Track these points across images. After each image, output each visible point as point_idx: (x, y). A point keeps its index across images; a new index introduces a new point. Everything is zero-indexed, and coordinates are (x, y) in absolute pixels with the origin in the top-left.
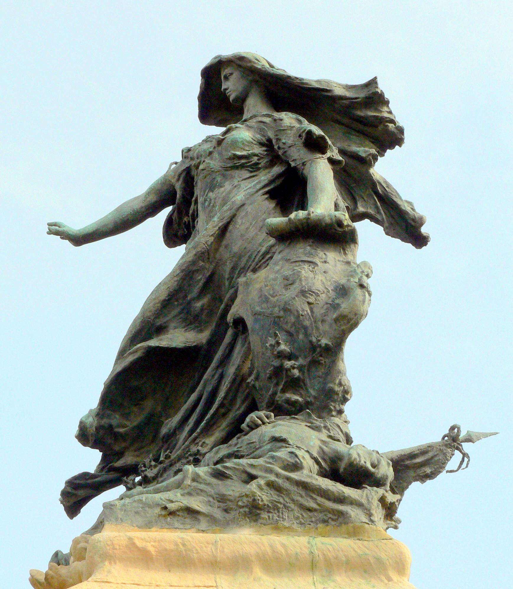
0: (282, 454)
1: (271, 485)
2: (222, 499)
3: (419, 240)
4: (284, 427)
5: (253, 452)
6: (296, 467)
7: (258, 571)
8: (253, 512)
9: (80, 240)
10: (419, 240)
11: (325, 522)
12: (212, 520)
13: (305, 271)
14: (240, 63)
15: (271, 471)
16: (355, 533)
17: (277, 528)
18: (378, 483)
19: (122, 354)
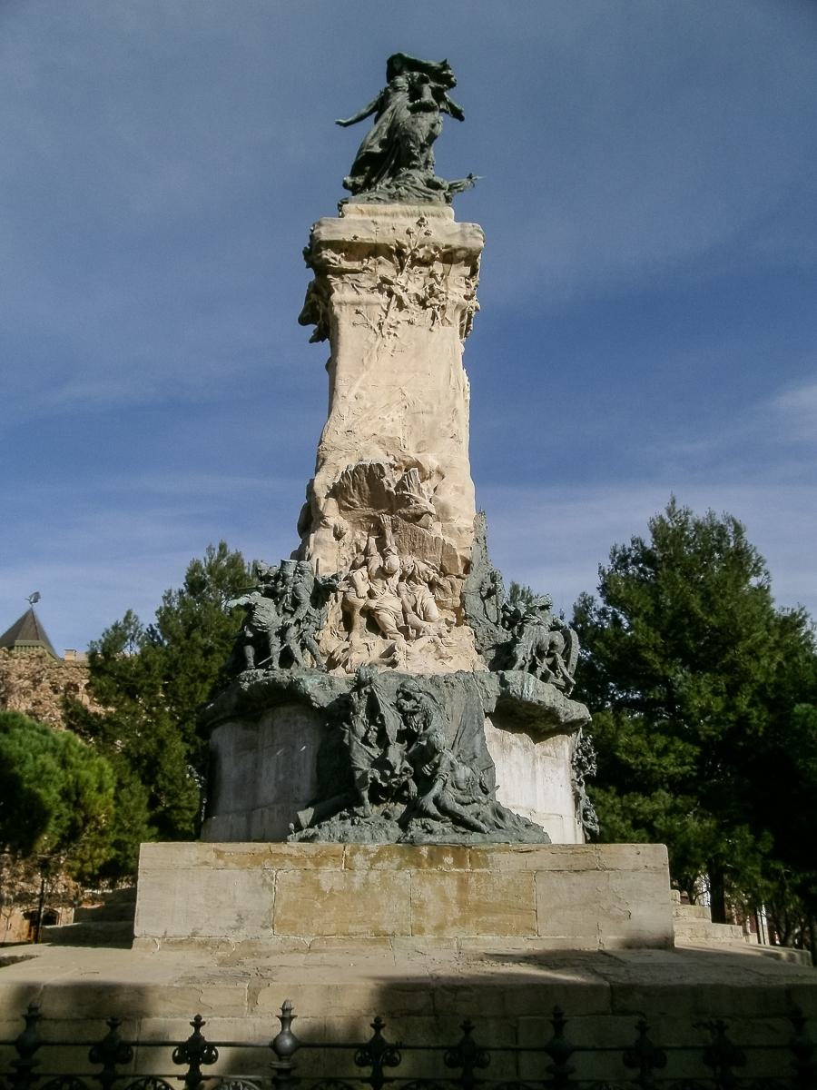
0: (410, 178)
1: (406, 188)
2: (389, 194)
3: (461, 119)
4: (413, 172)
5: (399, 179)
6: (414, 182)
7: (401, 217)
8: (400, 198)
9: (346, 125)
10: (461, 119)
11: (424, 201)
12: (385, 201)
13: (419, 120)
14: (400, 56)
15: (405, 184)
16: (434, 204)
17: (408, 203)
18: (443, 189)
19: (359, 154)
